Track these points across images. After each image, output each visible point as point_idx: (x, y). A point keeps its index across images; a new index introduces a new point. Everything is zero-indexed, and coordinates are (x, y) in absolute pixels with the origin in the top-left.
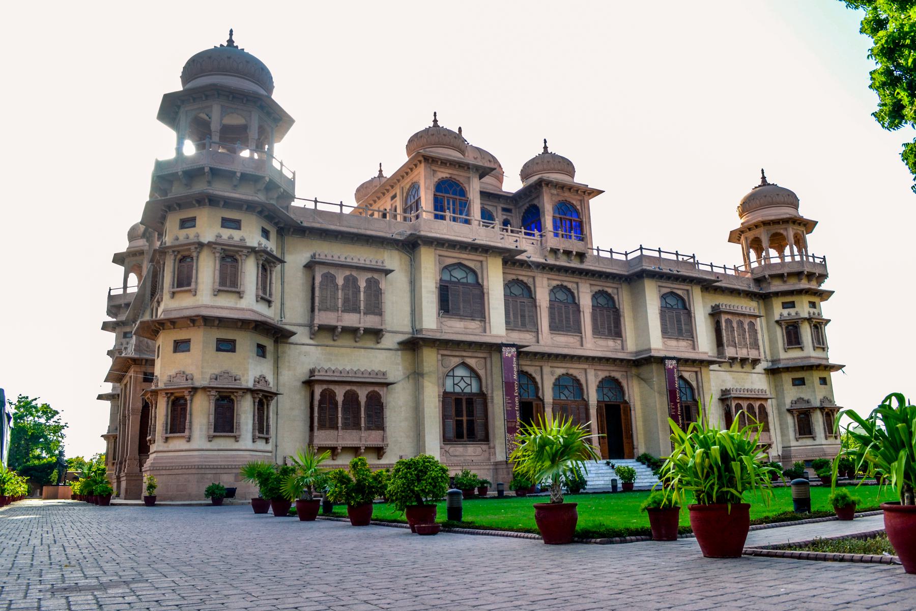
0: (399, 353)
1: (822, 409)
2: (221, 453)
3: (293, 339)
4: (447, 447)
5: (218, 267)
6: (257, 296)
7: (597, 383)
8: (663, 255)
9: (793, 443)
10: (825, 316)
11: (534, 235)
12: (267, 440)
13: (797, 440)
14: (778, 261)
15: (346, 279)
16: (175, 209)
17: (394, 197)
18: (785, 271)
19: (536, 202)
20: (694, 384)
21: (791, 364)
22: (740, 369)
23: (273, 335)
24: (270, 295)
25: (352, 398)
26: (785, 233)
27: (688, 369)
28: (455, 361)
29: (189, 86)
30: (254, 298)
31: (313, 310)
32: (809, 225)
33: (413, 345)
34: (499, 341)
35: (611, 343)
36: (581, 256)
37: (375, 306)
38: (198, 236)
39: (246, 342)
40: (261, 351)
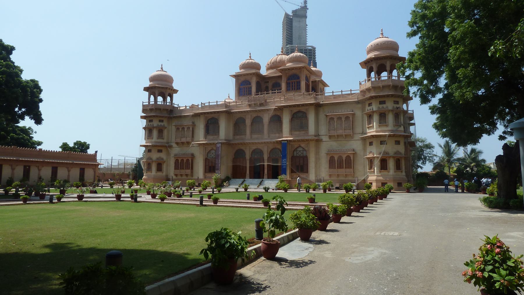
1: (393, 157)
4: (206, 174)
7: (269, 151)
20: (306, 149)
28: (210, 149)
35: (277, 135)
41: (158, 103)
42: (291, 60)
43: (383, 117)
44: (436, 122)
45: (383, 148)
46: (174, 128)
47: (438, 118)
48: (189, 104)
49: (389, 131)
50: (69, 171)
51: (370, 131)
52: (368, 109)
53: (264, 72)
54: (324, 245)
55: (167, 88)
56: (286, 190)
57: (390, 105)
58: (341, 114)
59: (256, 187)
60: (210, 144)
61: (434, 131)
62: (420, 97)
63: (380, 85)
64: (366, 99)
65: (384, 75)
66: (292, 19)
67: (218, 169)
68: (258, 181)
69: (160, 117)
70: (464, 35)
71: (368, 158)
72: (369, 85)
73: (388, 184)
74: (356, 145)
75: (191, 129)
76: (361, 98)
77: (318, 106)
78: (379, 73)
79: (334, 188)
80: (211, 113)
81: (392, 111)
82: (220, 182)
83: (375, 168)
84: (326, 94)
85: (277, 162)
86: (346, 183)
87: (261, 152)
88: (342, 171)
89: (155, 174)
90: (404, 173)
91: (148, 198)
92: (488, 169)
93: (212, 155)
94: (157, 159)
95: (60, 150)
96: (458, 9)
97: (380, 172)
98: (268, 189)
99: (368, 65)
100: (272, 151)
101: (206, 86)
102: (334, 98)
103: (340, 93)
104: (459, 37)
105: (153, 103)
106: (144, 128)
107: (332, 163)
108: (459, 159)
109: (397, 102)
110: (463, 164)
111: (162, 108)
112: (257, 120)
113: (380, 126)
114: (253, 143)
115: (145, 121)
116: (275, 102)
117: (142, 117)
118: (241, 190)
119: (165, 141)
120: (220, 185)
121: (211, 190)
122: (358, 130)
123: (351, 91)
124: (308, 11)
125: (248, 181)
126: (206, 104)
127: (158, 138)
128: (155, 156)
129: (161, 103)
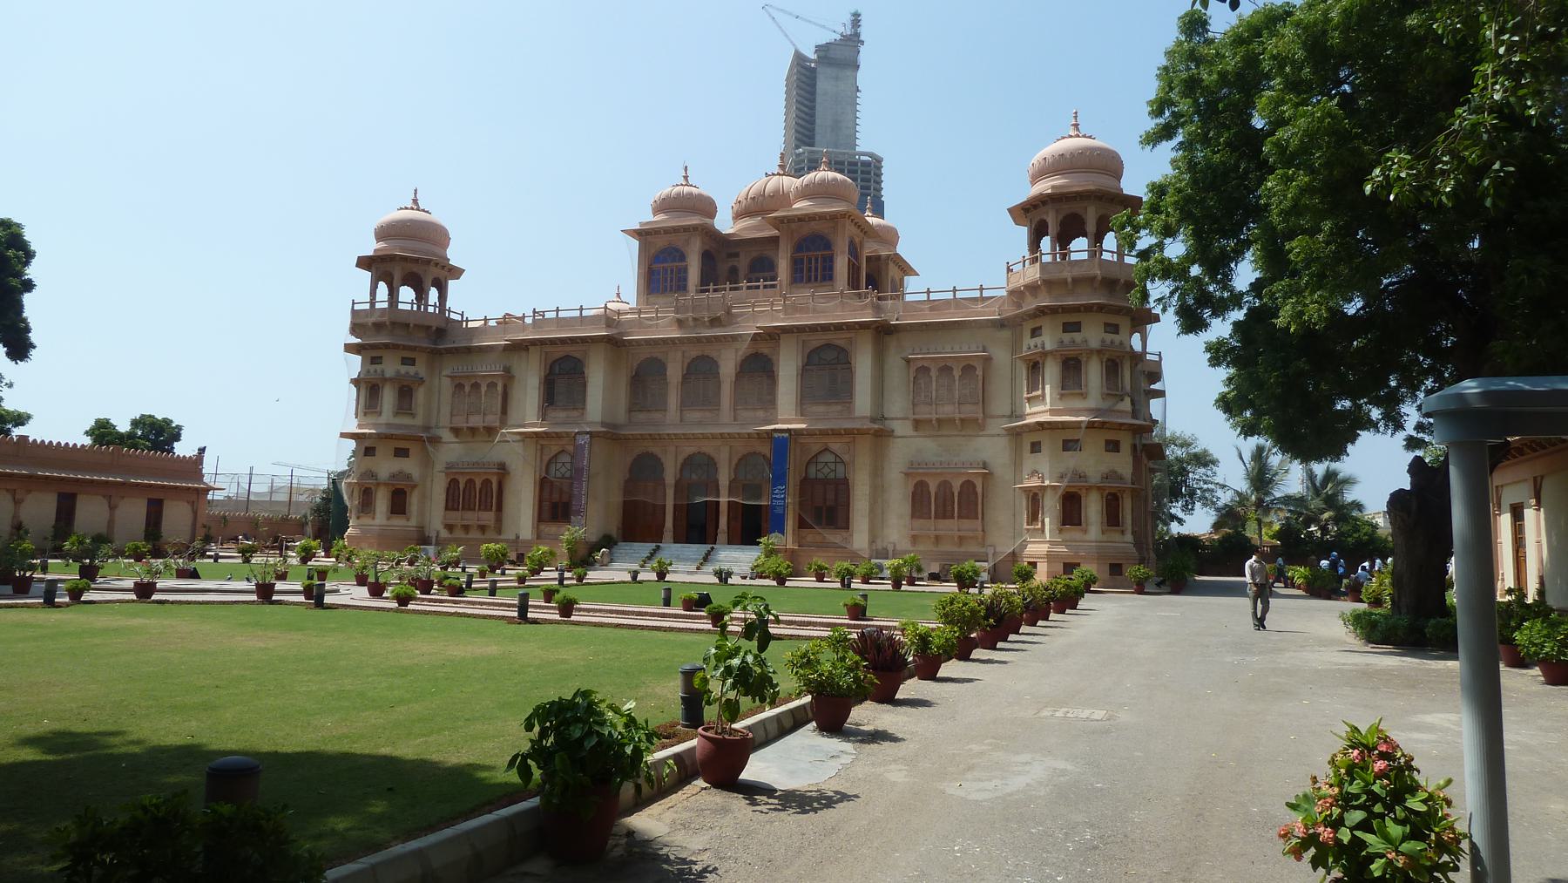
4: (542, 527)
20: (846, 458)
28: (555, 449)
35: (761, 414)
41: (401, 306)
42: (808, 192)
43: (1071, 368)
44: (1226, 390)
45: (1072, 461)
46: (447, 385)
47: (1230, 380)
48: (496, 314)
49: (1089, 411)
50: (112, 508)
51: (1035, 409)
52: (1029, 344)
53: (725, 223)
54: (886, 744)
55: (428, 262)
56: (781, 580)
57: (1093, 334)
58: (949, 357)
59: (693, 568)
60: (558, 436)
61: (1221, 416)
62: (1177, 313)
63: (1067, 274)
64: (1026, 314)
65: (1079, 246)
66: (813, 70)
67: (578, 513)
68: (698, 550)
69: (405, 348)
70: (1311, 138)
71: (1026, 490)
72: (1033, 274)
73: (1083, 568)
74: (991, 448)
75: (500, 388)
76: (1010, 311)
77: (883, 332)
78: (1063, 240)
79: (925, 575)
80: (563, 341)
81: (1099, 352)
82: (582, 552)
83: (1047, 520)
84: (908, 298)
85: (759, 497)
86: (960, 561)
87: (710, 463)
88: (950, 527)
89: (385, 522)
90: (1129, 537)
91: (360, 595)
92: (1367, 529)
93: (562, 469)
94: (393, 476)
95: (88, 441)
96: (1293, 62)
97: (1061, 531)
98: (729, 574)
99: (1032, 214)
100: (743, 462)
101: (547, 259)
102: (932, 309)
103: (950, 296)
104: (1295, 142)
105: (385, 305)
106: (356, 382)
107: (920, 501)
108: (1288, 500)
109: (1113, 328)
110: (1300, 514)
111: (412, 322)
112: (701, 370)
113: (1062, 396)
114: (686, 437)
115: (357, 360)
116: (755, 316)
117: (349, 348)
118: (648, 575)
119: (419, 421)
120: (583, 559)
121: (556, 575)
122: (1000, 405)
123: (981, 289)
124: (862, 49)
125: (670, 549)
126: (548, 315)
127: (396, 414)
128: (386, 466)
129: (408, 307)
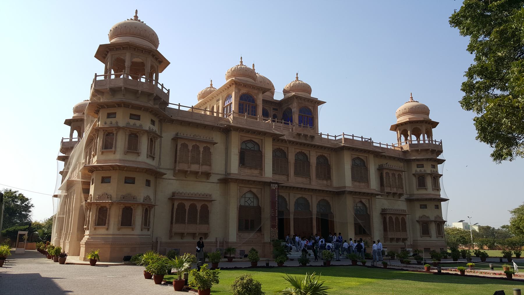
0: (218, 185)
2: (124, 236)
3: (164, 176)
5: (127, 140)
6: (147, 155)
8: (355, 138)
9: (419, 239)
10: (440, 173)
11: (288, 124)
12: (148, 230)
13: (421, 237)
14: (416, 142)
15: (193, 146)
16: (105, 108)
17: (218, 100)
18: (419, 148)
19: (290, 106)
20: (367, 205)
21: (419, 197)
22: (393, 198)
23: (154, 175)
24: (154, 154)
25: (193, 207)
26: (421, 128)
27: (364, 197)
28: (247, 190)
29: (113, 41)
30: (146, 156)
31: (175, 162)
32: (435, 124)
33: (226, 181)
34: (268, 181)
35: (325, 182)
36: (312, 137)
37: (208, 161)
38: (117, 123)
39: (140, 180)
40: (148, 183)
52: (415, 169)
